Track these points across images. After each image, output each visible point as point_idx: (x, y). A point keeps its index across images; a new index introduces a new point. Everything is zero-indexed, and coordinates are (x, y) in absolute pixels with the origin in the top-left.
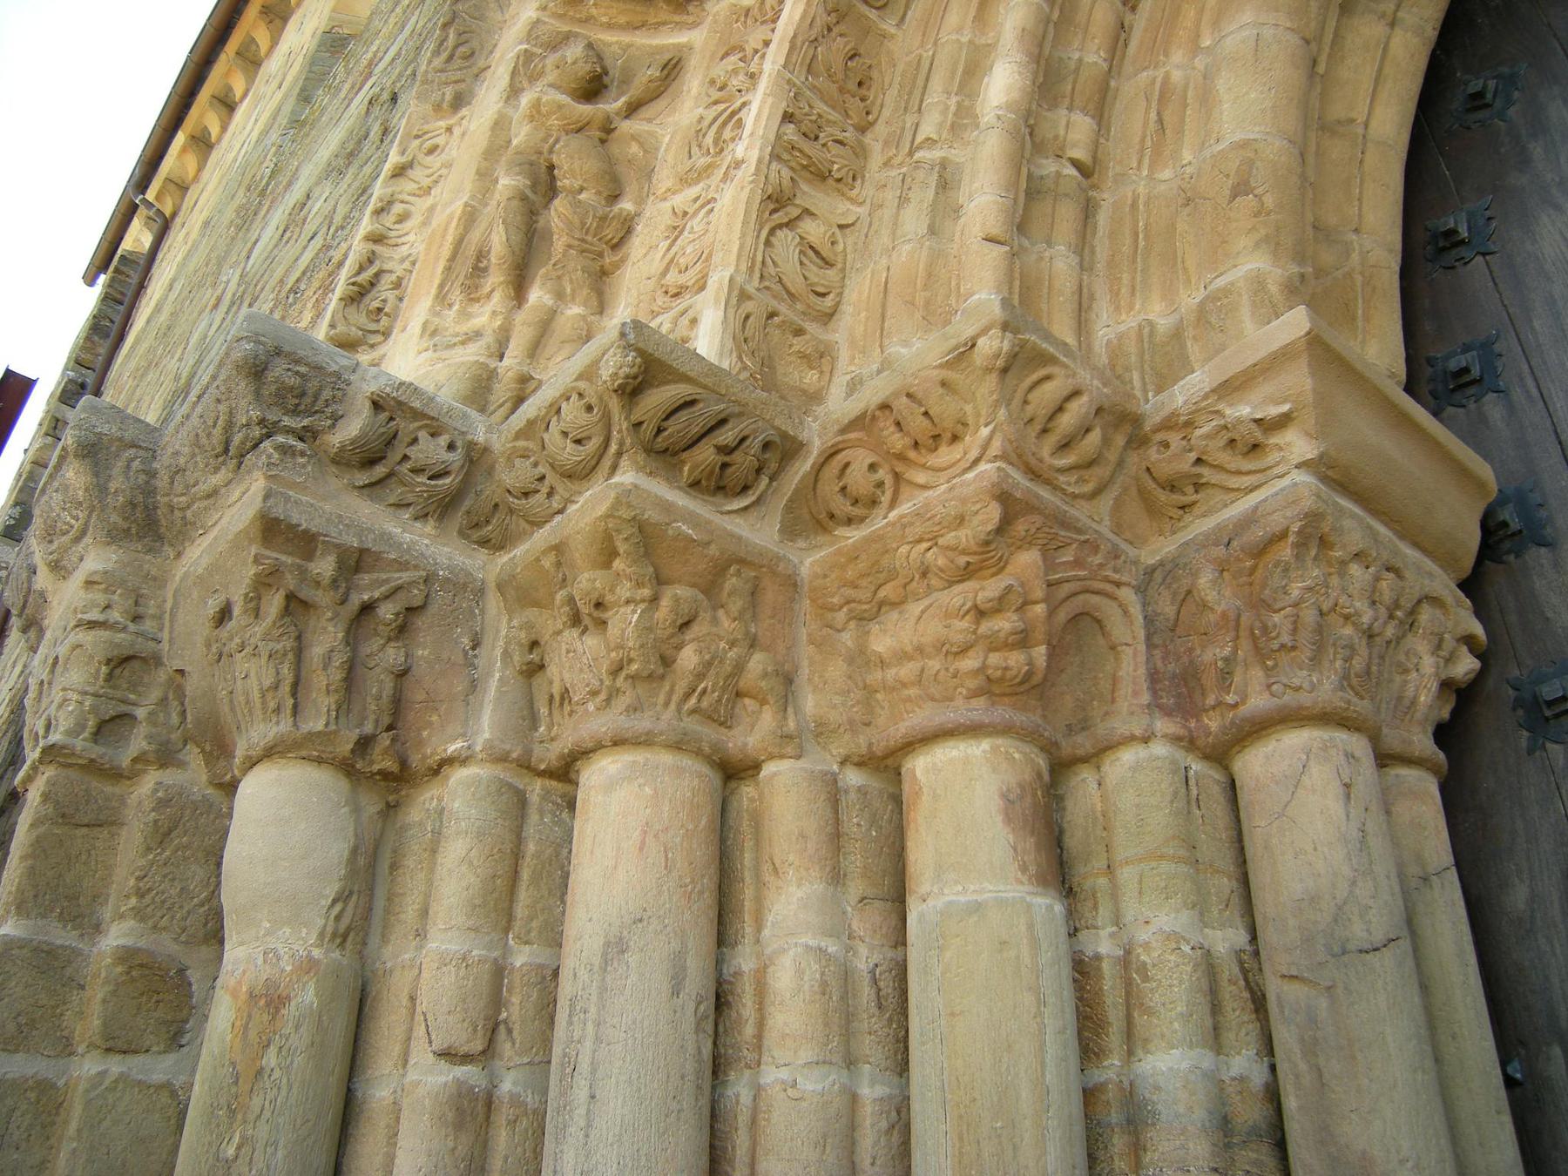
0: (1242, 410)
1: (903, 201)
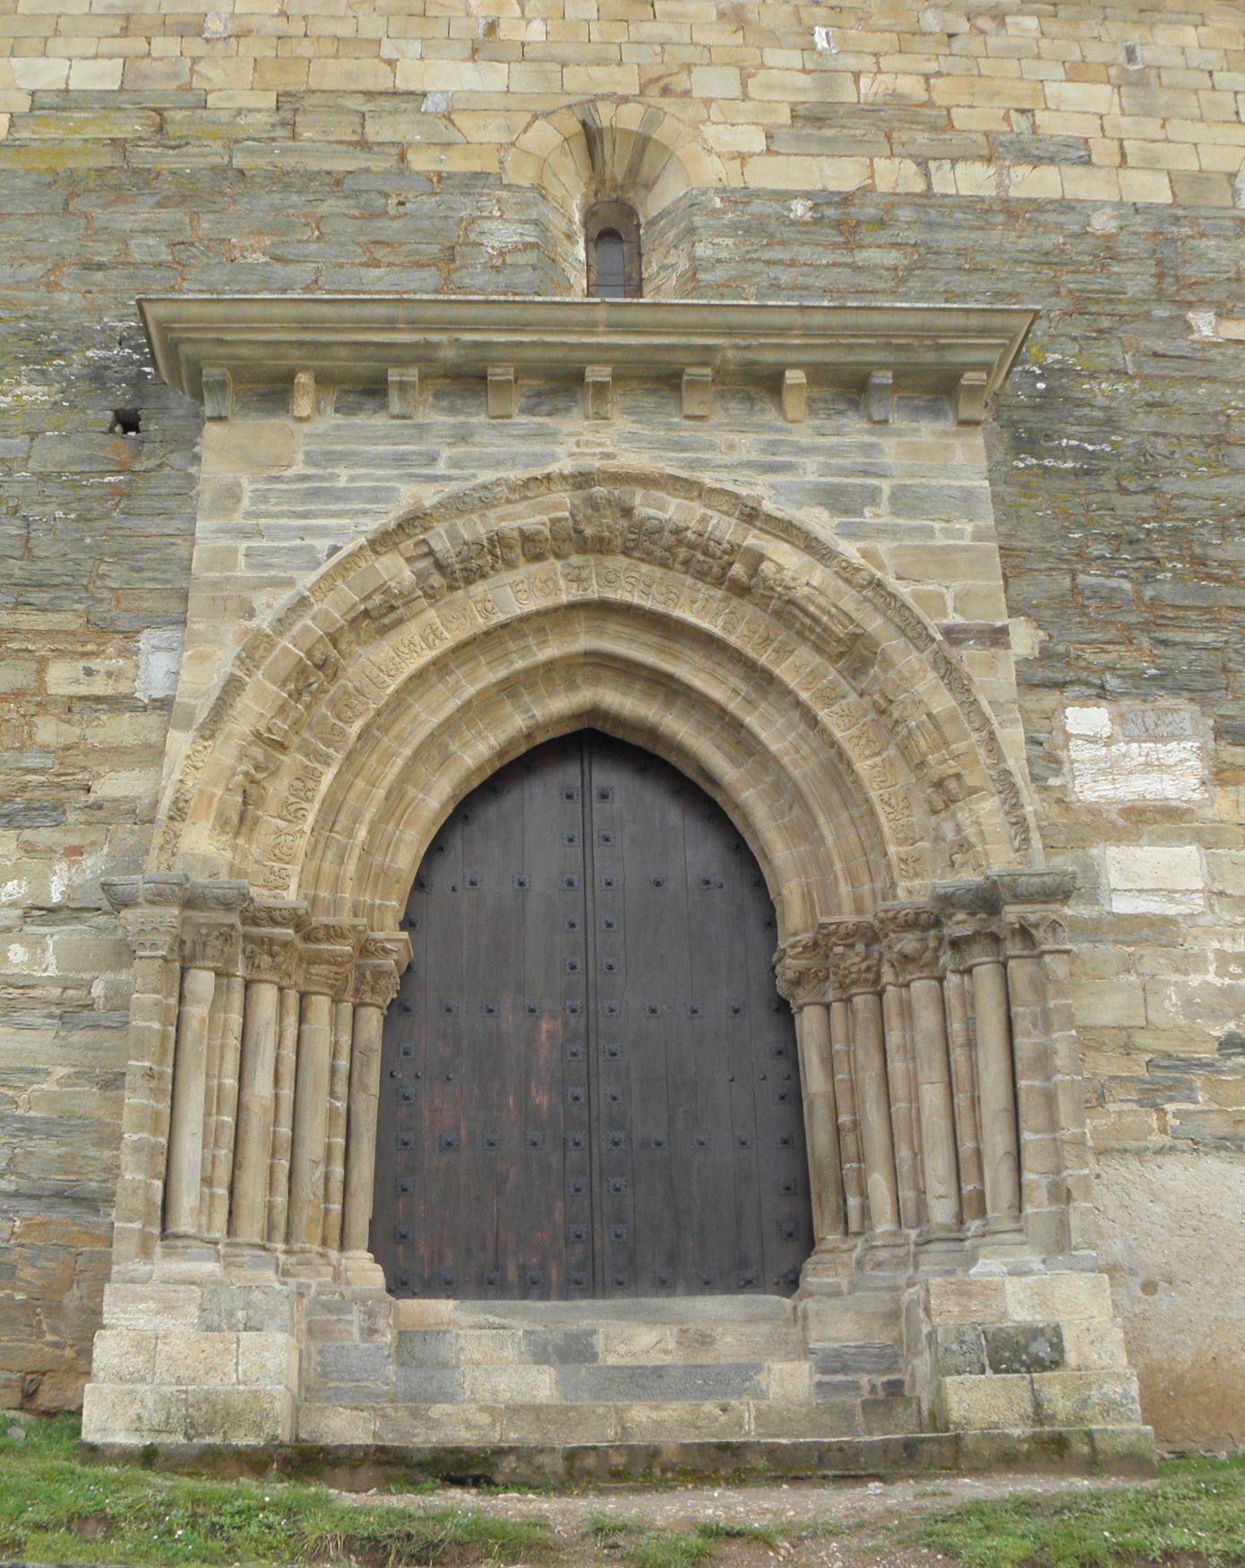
0: (389, 946)
1: (326, 847)
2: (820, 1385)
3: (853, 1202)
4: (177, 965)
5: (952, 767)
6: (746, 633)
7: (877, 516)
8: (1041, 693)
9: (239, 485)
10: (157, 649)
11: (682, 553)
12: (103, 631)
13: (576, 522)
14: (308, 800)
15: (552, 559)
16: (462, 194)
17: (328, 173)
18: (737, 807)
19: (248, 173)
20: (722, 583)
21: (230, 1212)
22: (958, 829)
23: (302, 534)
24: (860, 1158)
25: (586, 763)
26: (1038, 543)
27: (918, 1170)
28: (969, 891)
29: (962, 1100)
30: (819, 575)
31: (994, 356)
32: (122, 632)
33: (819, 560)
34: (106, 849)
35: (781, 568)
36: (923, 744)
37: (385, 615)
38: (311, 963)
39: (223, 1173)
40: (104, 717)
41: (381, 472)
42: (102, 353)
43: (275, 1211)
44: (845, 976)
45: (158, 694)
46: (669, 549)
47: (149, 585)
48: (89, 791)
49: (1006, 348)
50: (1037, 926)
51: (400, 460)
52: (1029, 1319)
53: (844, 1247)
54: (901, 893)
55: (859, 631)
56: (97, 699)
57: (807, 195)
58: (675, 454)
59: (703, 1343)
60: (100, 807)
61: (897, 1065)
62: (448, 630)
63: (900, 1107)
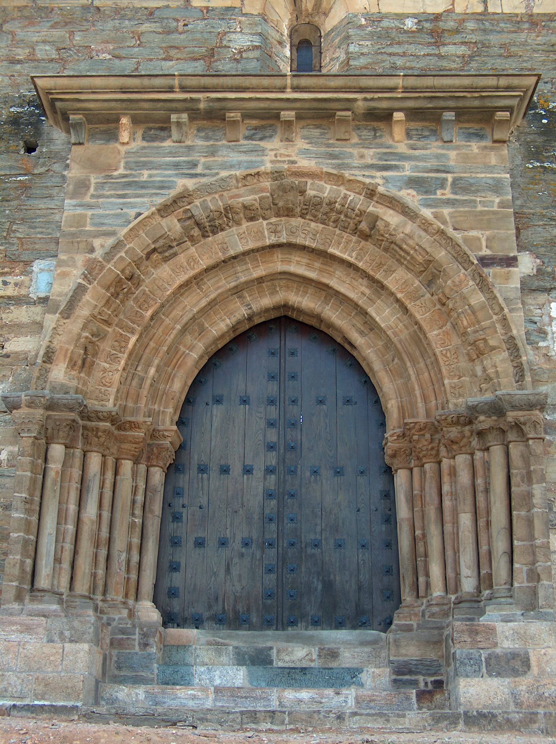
0: (166, 434)
1: (133, 379)
2: (395, 681)
3: (422, 579)
4: (43, 441)
5: (481, 334)
6: (368, 260)
7: (443, 194)
8: (535, 295)
9: (89, 180)
10: (42, 270)
11: (333, 216)
12: (14, 261)
13: (273, 199)
14: (121, 352)
15: (261, 220)
16: (219, 19)
17: (146, 8)
18: (364, 359)
19: (102, 9)
20: (356, 233)
21: (72, 578)
22: (484, 370)
23: (121, 206)
24: (426, 555)
25: (283, 334)
26: (538, 210)
27: (457, 562)
28: (486, 404)
29: (482, 522)
30: (410, 227)
31: (514, 102)
32: (24, 262)
33: (409, 219)
34: (11, 379)
35: (387, 225)
36: (465, 323)
37: (166, 251)
38: (122, 442)
39: (67, 556)
40: (12, 308)
41: (167, 172)
42: (19, 110)
43: (97, 578)
44: (419, 452)
45: (42, 295)
46: (326, 214)
47: (39, 236)
48: (3, 347)
49: (522, 98)
50: (525, 424)
51: (176, 166)
52: (511, 646)
53: (416, 604)
54: (451, 406)
55: (431, 259)
56: (9, 298)
57: (414, 16)
58: (330, 161)
59: (333, 656)
60: (8, 356)
61: (447, 503)
62: (202, 260)
63: (448, 527)
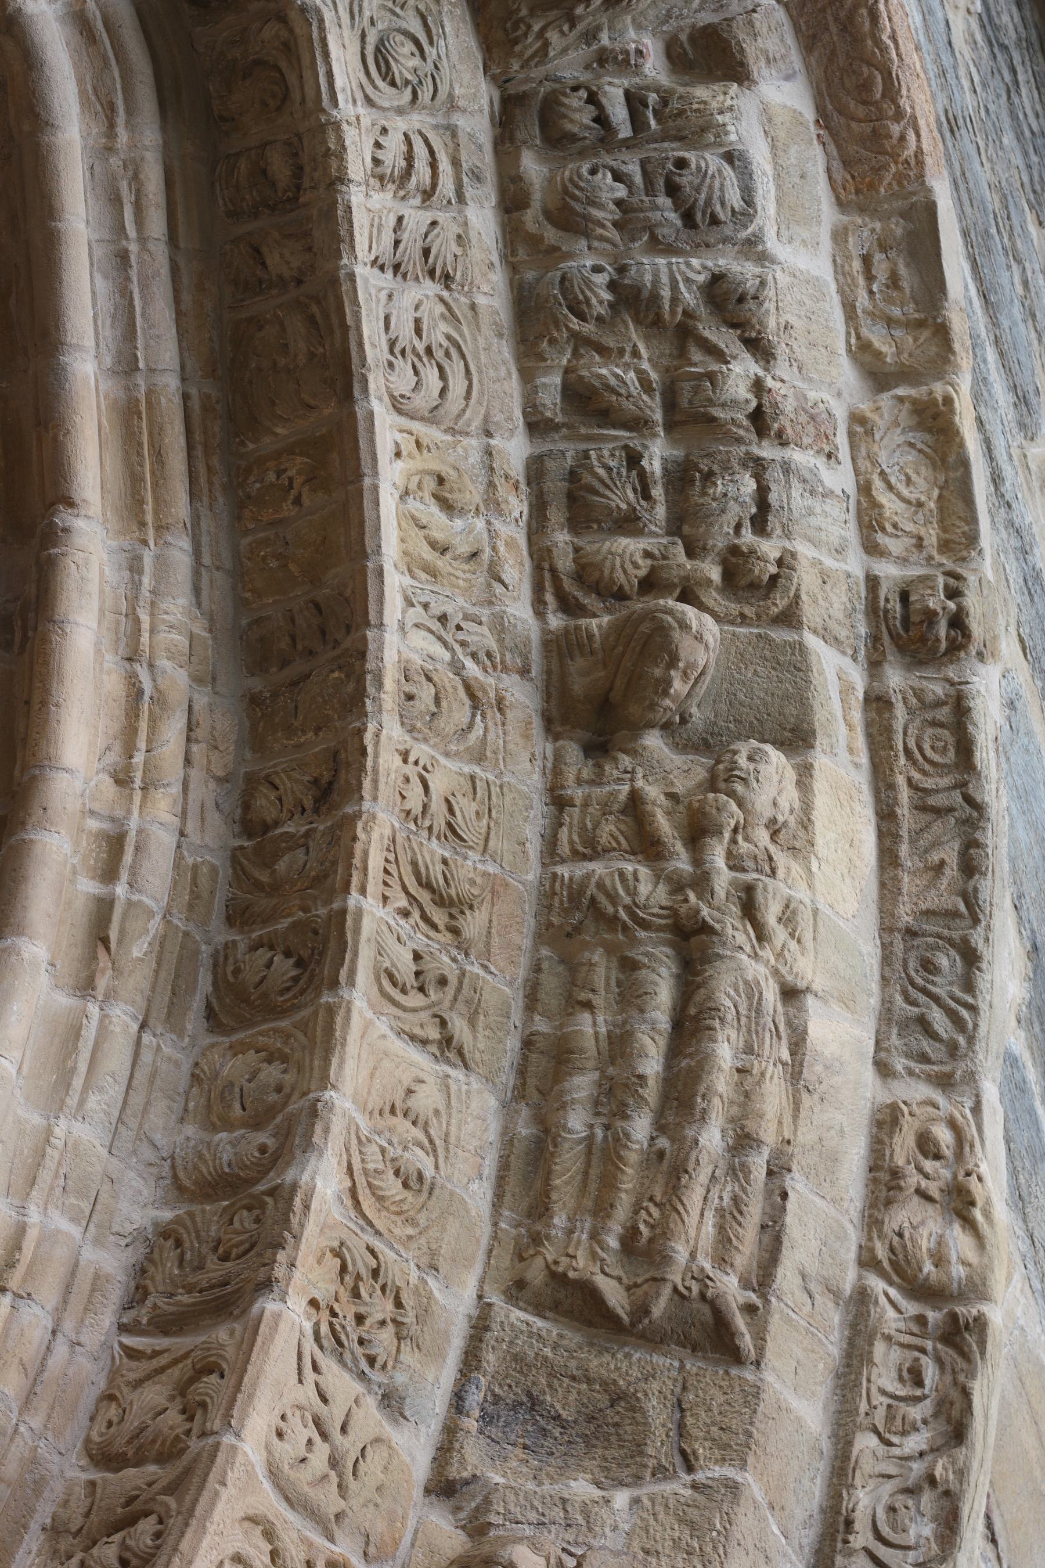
20: (568, 606)
33: (886, 1015)
